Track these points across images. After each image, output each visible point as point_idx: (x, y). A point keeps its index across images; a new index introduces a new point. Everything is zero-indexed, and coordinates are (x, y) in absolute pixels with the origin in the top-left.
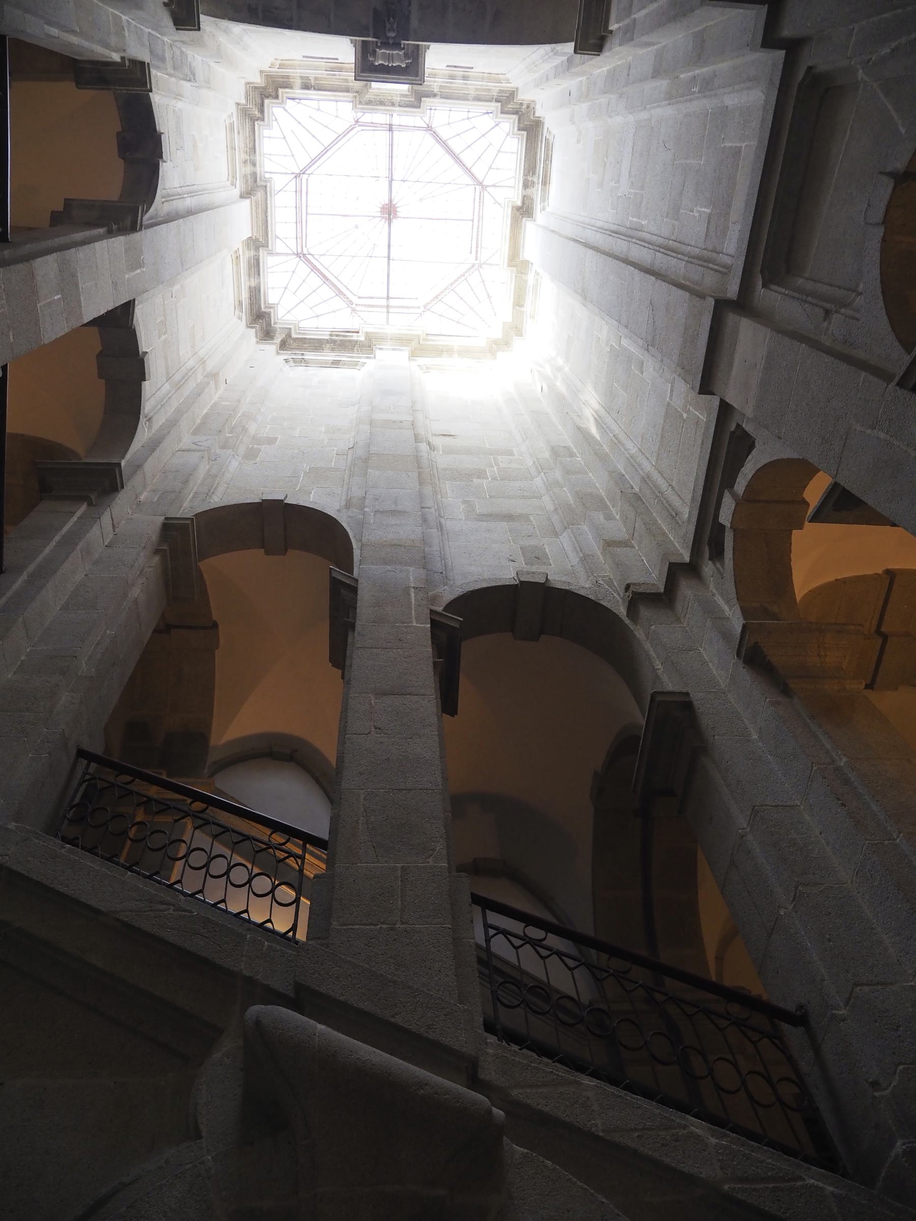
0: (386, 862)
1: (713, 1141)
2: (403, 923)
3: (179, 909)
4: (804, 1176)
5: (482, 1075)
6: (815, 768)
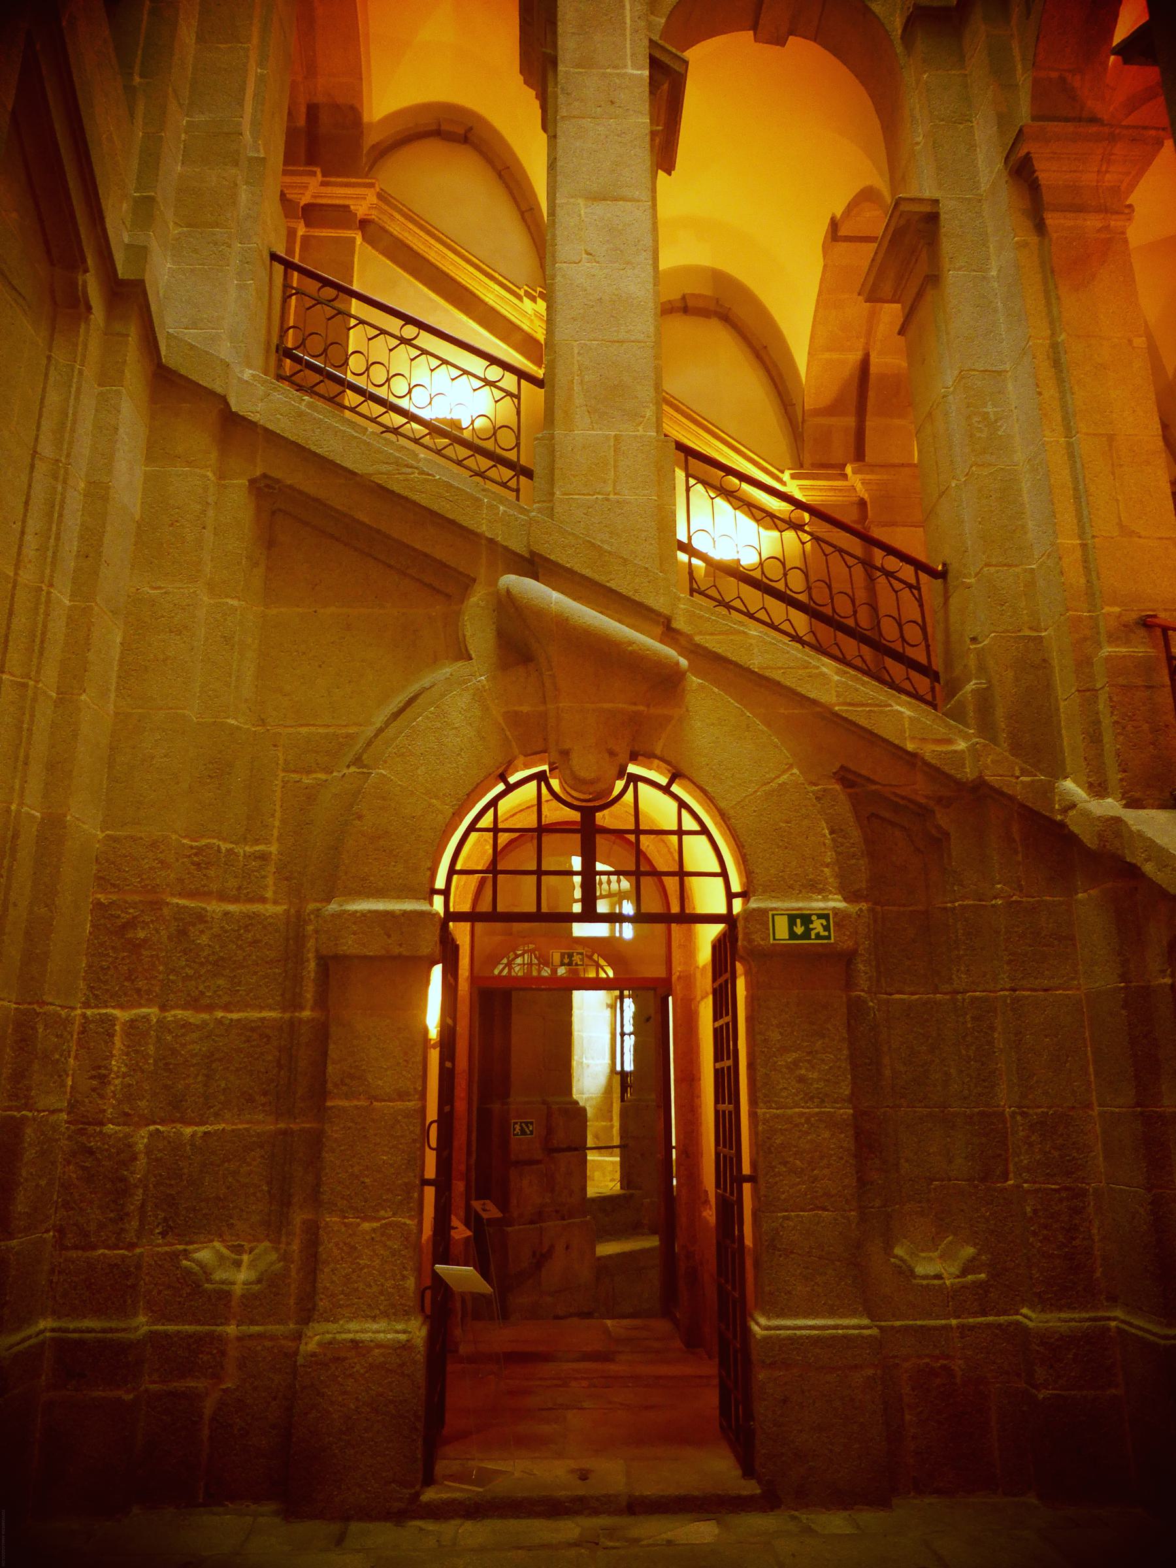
0: (601, 429)
1: (836, 678)
2: (615, 494)
3: (422, 473)
4: (893, 704)
5: (675, 625)
6: (1030, 343)
